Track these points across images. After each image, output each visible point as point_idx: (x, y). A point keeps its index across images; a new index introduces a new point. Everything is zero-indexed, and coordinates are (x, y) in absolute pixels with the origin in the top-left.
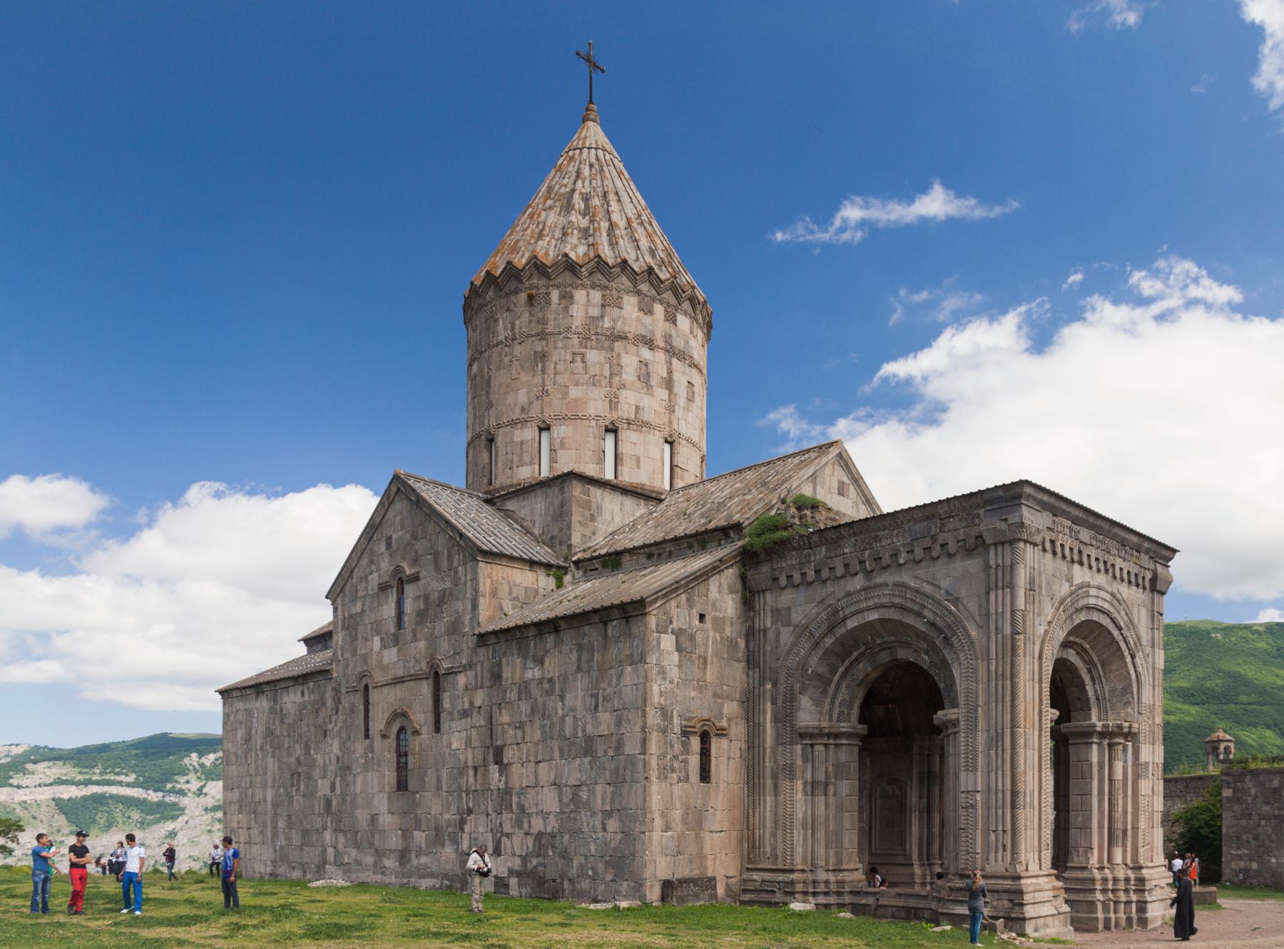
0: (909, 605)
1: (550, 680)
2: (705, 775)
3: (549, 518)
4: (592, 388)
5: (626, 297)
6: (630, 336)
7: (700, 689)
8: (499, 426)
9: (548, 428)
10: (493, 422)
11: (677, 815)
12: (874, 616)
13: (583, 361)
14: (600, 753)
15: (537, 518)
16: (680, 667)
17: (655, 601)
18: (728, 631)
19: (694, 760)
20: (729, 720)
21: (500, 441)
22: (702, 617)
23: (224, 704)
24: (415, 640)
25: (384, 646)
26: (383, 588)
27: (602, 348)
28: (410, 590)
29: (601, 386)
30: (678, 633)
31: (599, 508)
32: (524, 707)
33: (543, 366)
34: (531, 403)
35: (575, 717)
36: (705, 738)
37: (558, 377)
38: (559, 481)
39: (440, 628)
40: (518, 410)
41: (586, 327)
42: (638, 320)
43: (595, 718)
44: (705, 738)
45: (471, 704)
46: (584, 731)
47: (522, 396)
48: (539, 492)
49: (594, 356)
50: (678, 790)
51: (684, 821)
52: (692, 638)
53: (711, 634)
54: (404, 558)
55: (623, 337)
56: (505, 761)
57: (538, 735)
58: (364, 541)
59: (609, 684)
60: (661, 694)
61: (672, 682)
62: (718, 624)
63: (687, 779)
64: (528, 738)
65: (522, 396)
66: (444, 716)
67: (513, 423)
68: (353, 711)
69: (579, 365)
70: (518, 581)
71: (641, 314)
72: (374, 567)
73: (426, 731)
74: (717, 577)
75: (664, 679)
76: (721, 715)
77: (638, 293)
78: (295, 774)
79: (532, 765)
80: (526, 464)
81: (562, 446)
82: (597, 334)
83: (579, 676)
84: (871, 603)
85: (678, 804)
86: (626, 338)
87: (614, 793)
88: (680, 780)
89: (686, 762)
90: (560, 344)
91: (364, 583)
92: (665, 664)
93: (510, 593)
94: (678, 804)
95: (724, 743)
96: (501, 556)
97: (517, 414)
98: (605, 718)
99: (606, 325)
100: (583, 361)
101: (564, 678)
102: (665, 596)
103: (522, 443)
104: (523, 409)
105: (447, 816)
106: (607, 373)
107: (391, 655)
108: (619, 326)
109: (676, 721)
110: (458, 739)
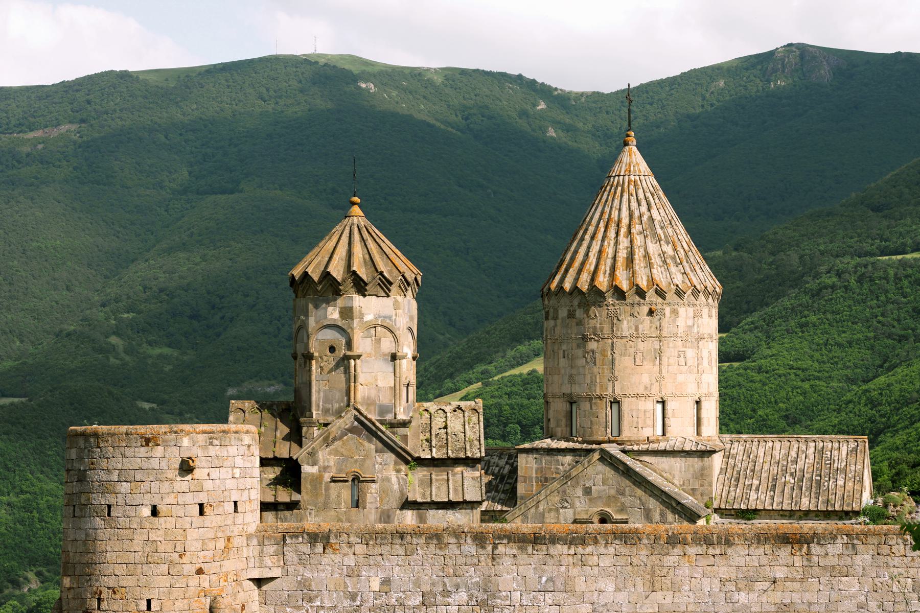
3: (690, 476)
15: (677, 473)
33: (661, 360)
34: (652, 384)
47: (645, 379)
54: (609, 506)
67: (637, 396)
69: (682, 360)
72: (566, 504)
81: (674, 416)
90: (671, 345)
91: (553, 514)
97: (641, 390)
103: (645, 411)
104: (646, 388)
106: (696, 364)
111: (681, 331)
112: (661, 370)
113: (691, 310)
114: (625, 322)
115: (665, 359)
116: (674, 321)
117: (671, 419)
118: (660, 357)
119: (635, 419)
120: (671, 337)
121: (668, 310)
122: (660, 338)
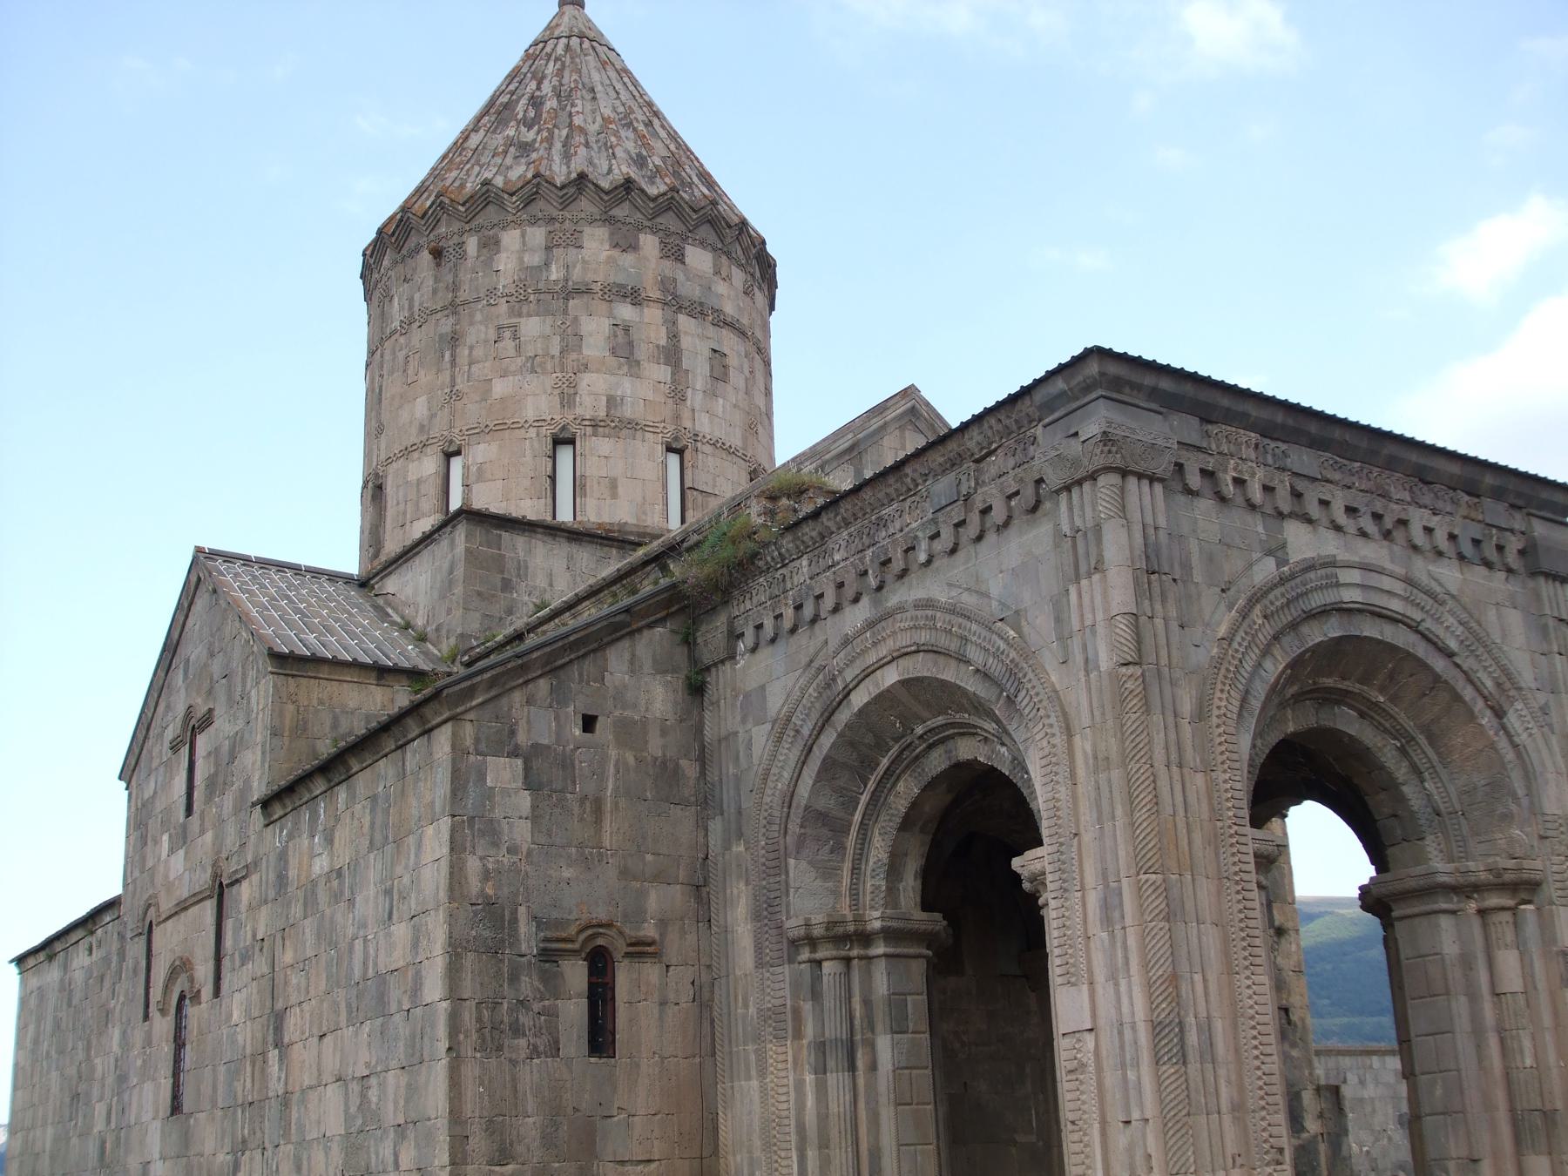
0: (943, 641)
1: (339, 873)
2: (600, 1038)
4: (529, 377)
5: (587, 230)
6: (597, 288)
7: (586, 863)
8: (389, 461)
9: (458, 453)
10: (383, 457)
11: (530, 1126)
12: (890, 677)
13: (515, 337)
14: (393, 1008)
16: (535, 818)
17: (470, 692)
18: (655, 746)
19: (574, 1011)
20: (663, 923)
21: (389, 489)
22: (589, 723)
23: (23, 983)
24: (202, 832)
25: (172, 851)
26: (175, 748)
27: (548, 312)
28: (202, 742)
29: (544, 372)
30: (531, 757)
31: (522, 570)
32: (309, 927)
35: (365, 940)
36: (600, 963)
37: (474, 368)
38: (449, 529)
39: (228, 801)
40: (414, 430)
41: (521, 284)
42: (610, 261)
43: (389, 935)
44: (600, 963)
45: (254, 936)
46: (376, 964)
48: (425, 553)
49: (532, 326)
50: (531, 1075)
51: (548, 1140)
52: (566, 764)
53: (613, 753)
55: (584, 291)
56: (286, 1040)
57: (323, 986)
58: (162, 674)
59: (406, 867)
60: (486, 875)
61: (512, 850)
62: (630, 733)
63: (554, 1049)
64: (312, 992)
65: (420, 408)
66: (226, 963)
67: (407, 452)
68: (135, 971)
69: (508, 345)
70: (352, 705)
71: (616, 253)
73: (207, 993)
74: (626, 643)
75: (496, 845)
76: (639, 915)
77: (609, 220)
78: (76, 1097)
79: (316, 1039)
80: (424, 515)
82: (537, 291)
83: (372, 856)
84: (883, 650)
85: (531, 1106)
86: (588, 291)
87: (409, 1085)
88: (535, 1052)
89: (552, 1014)
90: (478, 317)
92: (498, 814)
93: (335, 726)
94: (531, 1106)
95: (651, 972)
96: (316, 661)
98: (401, 931)
99: (554, 277)
100: (515, 337)
101: (354, 865)
102: (492, 683)
103: (419, 482)
104: (422, 427)
105: (221, 1157)
106: (555, 351)
107: (178, 862)
108: (577, 274)
109: (525, 928)
110: (241, 999)
111: (504, 282)
112: (453, 378)
113: (538, 235)
114: (396, 299)
115: (463, 352)
116: (488, 263)
117: (475, 488)
118: (454, 348)
119: (402, 506)
120: (478, 300)
121: (472, 244)
122: (453, 308)
